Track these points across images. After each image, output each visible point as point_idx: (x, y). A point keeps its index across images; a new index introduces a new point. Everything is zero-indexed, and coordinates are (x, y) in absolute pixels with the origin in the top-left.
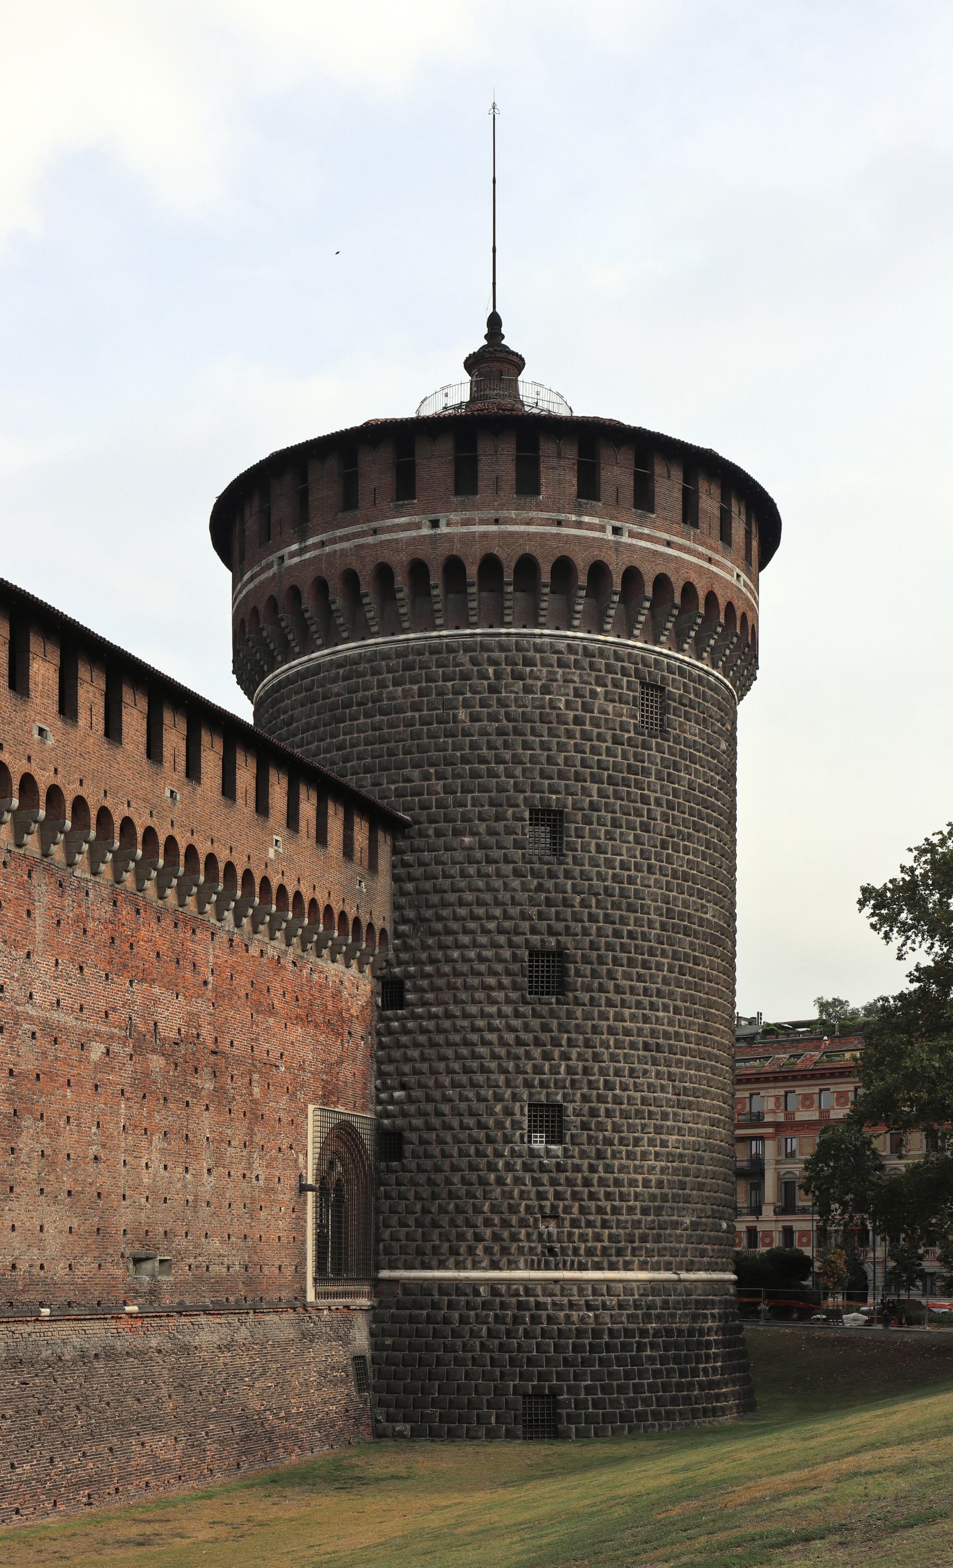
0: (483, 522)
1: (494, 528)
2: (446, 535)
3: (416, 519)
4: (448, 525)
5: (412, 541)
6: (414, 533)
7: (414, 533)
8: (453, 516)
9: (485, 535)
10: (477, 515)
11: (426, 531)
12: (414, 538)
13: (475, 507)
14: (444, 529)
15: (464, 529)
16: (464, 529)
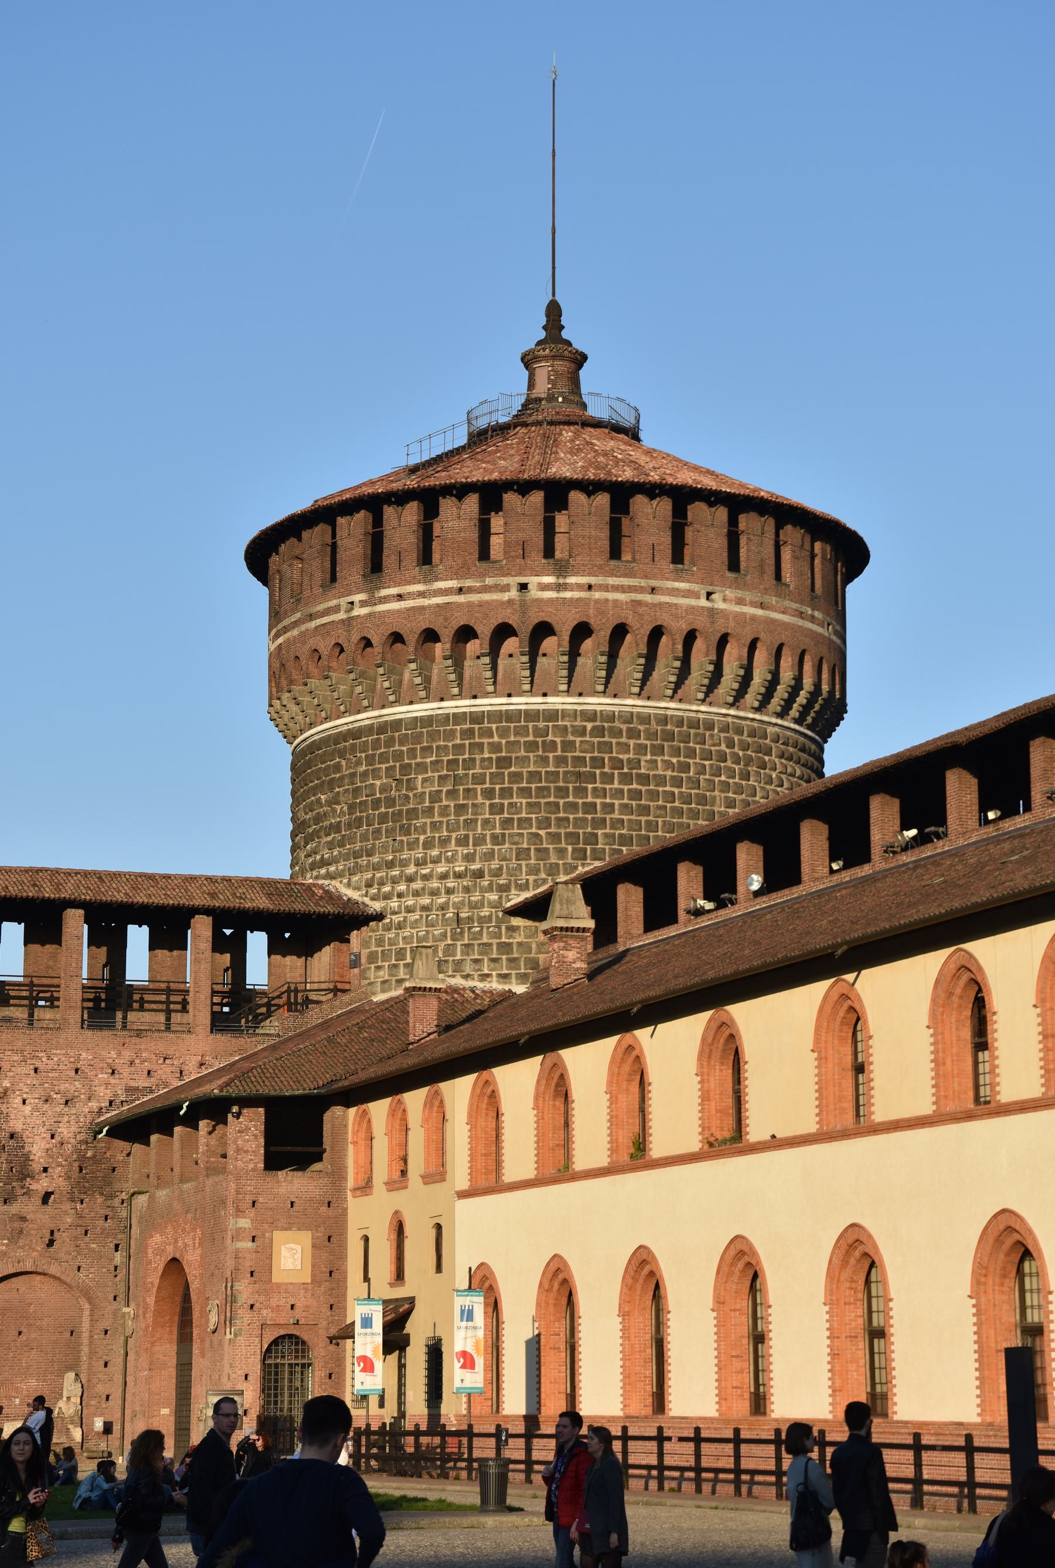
0: (753, 604)
1: (760, 612)
2: (722, 611)
3: (695, 587)
4: (724, 600)
5: (692, 609)
6: (693, 602)
7: (693, 602)
8: (728, 593)
9: (753, 618)
10: (748, 596)
11: (703, 602)
12: (693, 607)
13: (744, 587)
14: (721, 605)
15: (738, 609)
16: (738, 609)
